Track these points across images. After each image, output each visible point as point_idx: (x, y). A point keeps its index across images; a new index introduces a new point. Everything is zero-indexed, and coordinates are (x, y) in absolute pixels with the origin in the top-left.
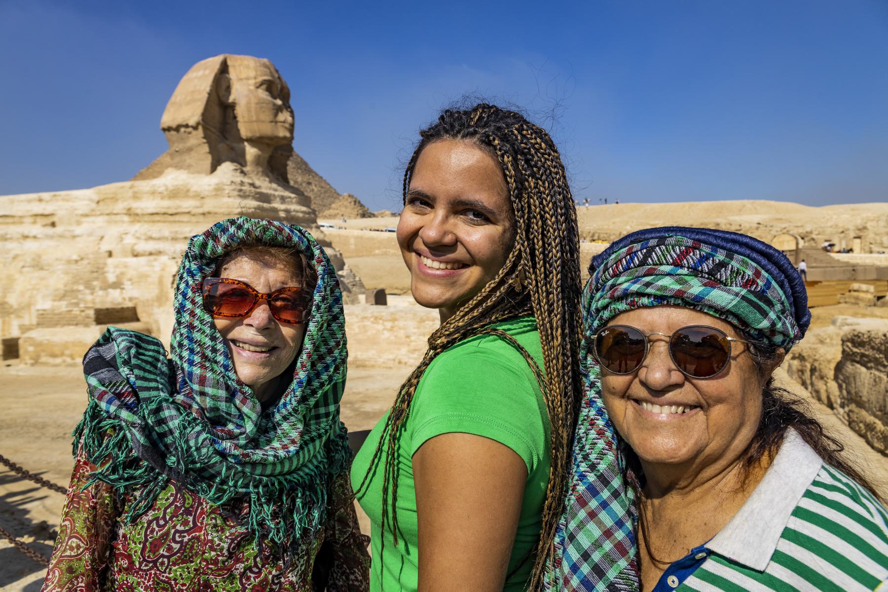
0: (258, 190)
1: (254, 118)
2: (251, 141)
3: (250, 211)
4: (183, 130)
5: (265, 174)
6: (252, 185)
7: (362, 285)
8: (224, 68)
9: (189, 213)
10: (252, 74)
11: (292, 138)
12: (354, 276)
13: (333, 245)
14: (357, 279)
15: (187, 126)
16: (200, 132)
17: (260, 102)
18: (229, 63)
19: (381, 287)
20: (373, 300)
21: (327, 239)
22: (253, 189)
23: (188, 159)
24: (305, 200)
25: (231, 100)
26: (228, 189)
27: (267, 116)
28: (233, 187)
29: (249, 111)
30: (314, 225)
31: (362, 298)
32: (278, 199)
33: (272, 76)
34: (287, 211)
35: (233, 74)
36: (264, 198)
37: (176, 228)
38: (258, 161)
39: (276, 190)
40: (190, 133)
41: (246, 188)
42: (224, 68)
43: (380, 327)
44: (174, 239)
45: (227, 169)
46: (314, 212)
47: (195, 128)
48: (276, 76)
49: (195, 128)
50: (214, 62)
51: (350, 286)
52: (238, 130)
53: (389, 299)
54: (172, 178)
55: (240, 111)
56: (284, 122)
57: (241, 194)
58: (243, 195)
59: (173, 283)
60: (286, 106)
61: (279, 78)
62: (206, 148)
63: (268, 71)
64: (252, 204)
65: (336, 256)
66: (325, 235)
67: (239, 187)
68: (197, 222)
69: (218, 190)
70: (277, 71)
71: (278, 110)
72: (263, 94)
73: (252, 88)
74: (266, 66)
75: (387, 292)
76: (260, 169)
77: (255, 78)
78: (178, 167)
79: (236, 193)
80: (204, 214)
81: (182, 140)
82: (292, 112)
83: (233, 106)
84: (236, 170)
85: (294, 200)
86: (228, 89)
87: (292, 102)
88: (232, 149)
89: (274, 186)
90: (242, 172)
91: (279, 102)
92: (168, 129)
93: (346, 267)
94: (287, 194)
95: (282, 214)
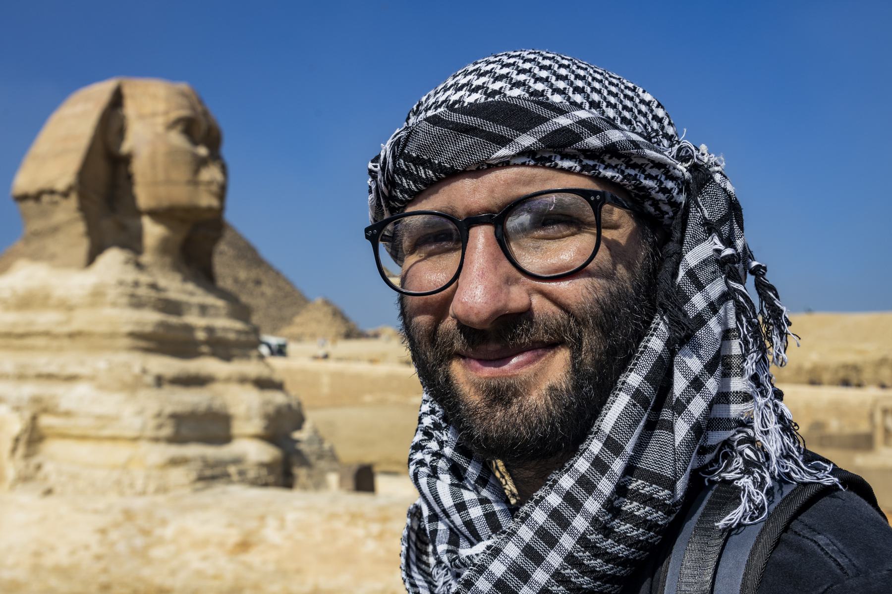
0: (163, 295)
1: (161, 176)
2: (157, 215)
3: (148, 329)
4: (46, 198)
5: (176, 267)
6: (154, 286)
7: (333, 457)
8: (117, 100)
9: (47, 334)
10: (161, 107)
11: (221, 210)
12: (321, 441)
13: (288, 386)
14: (326, 446)
15: (52, 192)
16: (73, 202)
17: (172, 153)
18: (127, 91)
19: (368, 459)
20: (350, 483)
21: (277, 377)
22: (153, 294)
23: (53, 245)
24: (240, 311)
25: (126, 147)
26: (112, 293)
27: (182, 174)
28: (121, 290)
29: (153, 165)
30: (254, 353)
31: (333, 479)
32: (195, 311)
33: (193, 108)
34: (210, 330)
35: (130, 109)
36: (172, 307)
37: (24, 358)
38: (164, 247)
39: (192, 294)
40: (55, 203)
41: (143, 291)
42: (117, 100)
43: (359, 532)
44: (21, 377)
45: (113, 260)
46: (256, 331)
47: (65, 194)
48: (199, 109)
49: (65, 194)
50: (102, 91)
51: (312, 459)
52: (133, 198)
53: (382, 483)
54: (25, 275)
55: (140, 168)
56: (210, 183)
57: (134, 300)
58: (137, 303)
59: (14, 450)
60: (215, 156)
61: (206, 114)
62: (80, 227)
63: (184, 102)
64: (150, 318)
65: (289, 407)
66: (272, 369)
67: (129, 290)
68: (60, 349)
69: (97, 296)
70: (201, 102)
71: (200, 163)
72: (177, 139)
73: (160, 129)
74: (183, 95)
75: (377, 469)
76: (168, 260)
77: (166, 113)
78: (35, 257)
79: (125, 300)
80: (72, 336)
81: (44, 214)
82: (224, 169)
83: (127, 160)
84: (127, 262)
85: (224, 312)
86: (121, 133)
87: (226, 151)
88: (123, 228)
89: (190, 287)
90: (139, 266)
91: (203, 151)
92: (23, 198)
93: (308, 426)
94: (210, 300)
95: (201, 335)
